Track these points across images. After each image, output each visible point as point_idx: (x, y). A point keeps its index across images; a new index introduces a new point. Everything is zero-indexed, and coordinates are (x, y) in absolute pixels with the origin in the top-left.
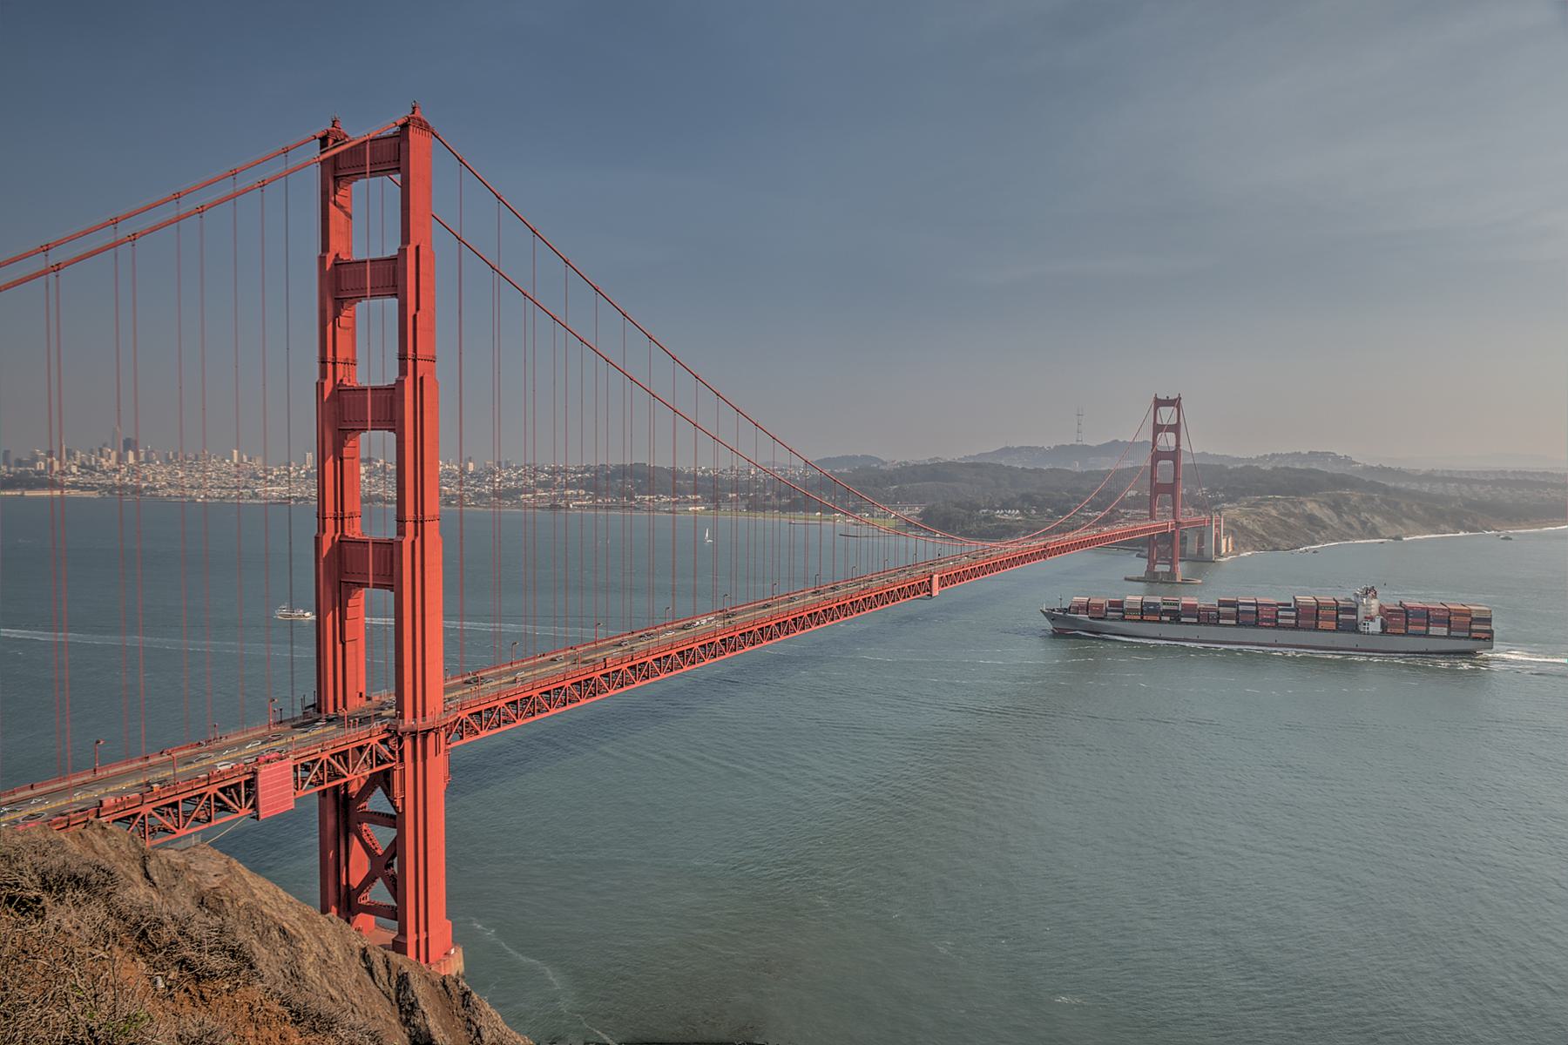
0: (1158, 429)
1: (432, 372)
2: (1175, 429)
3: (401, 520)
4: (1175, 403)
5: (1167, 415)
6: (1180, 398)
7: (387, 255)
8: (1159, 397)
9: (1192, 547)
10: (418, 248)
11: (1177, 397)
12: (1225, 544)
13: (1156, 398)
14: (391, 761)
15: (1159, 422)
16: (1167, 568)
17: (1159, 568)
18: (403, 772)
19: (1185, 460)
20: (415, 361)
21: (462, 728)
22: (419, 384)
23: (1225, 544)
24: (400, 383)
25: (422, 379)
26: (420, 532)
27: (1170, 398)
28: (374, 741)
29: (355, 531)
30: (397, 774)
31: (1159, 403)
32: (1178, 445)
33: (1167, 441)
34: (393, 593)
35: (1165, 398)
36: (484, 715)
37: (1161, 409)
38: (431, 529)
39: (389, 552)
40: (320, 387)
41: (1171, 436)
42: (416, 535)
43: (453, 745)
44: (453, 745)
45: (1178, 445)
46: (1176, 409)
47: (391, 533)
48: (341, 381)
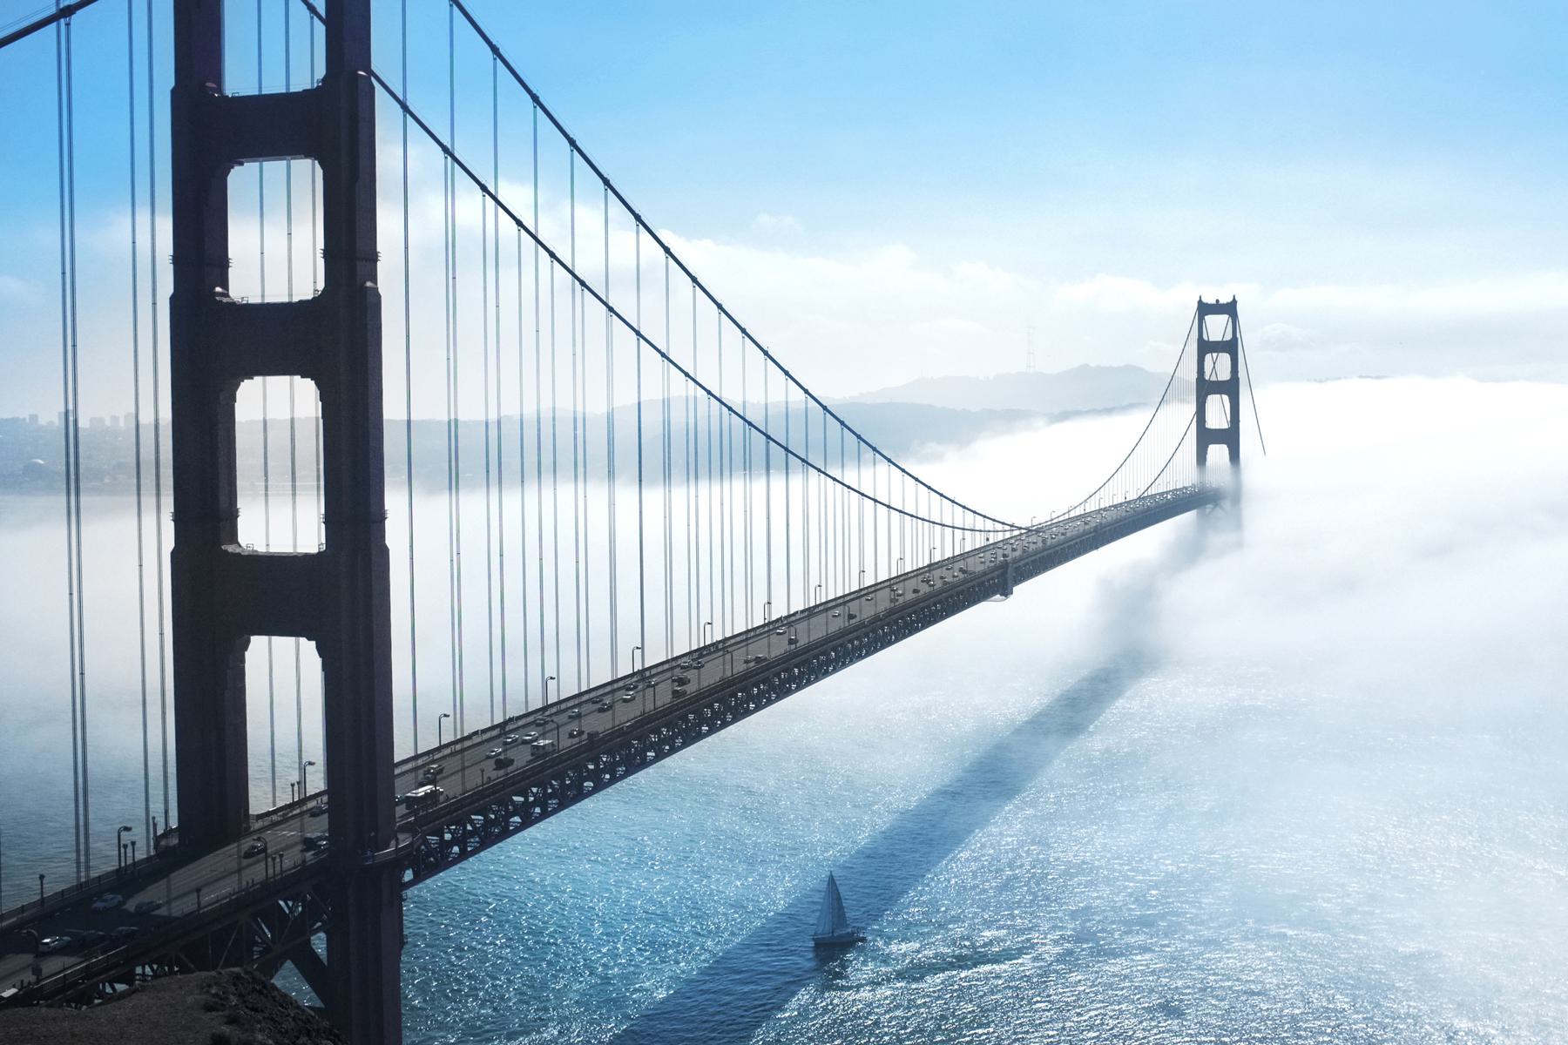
0: (1205, 347)
1: (373, 277)
2: (1230, 347)
3: (332, 519)
4: (1230, 309)
5: (1217, 327)
6: (1236, 302)
7: (296, 87)
8: (1204, 300)
11: (1230, 300)
13: (1200, 302)
15: (1206, 339)
27: (1223, 301)
31: (1204, 309)
33: (1219, 367)
34: (313, 643)
35: (1214, 302)
36: (448, 836)
37: (1210, 319)
41: (1225, 358)
46: (1230, 323)
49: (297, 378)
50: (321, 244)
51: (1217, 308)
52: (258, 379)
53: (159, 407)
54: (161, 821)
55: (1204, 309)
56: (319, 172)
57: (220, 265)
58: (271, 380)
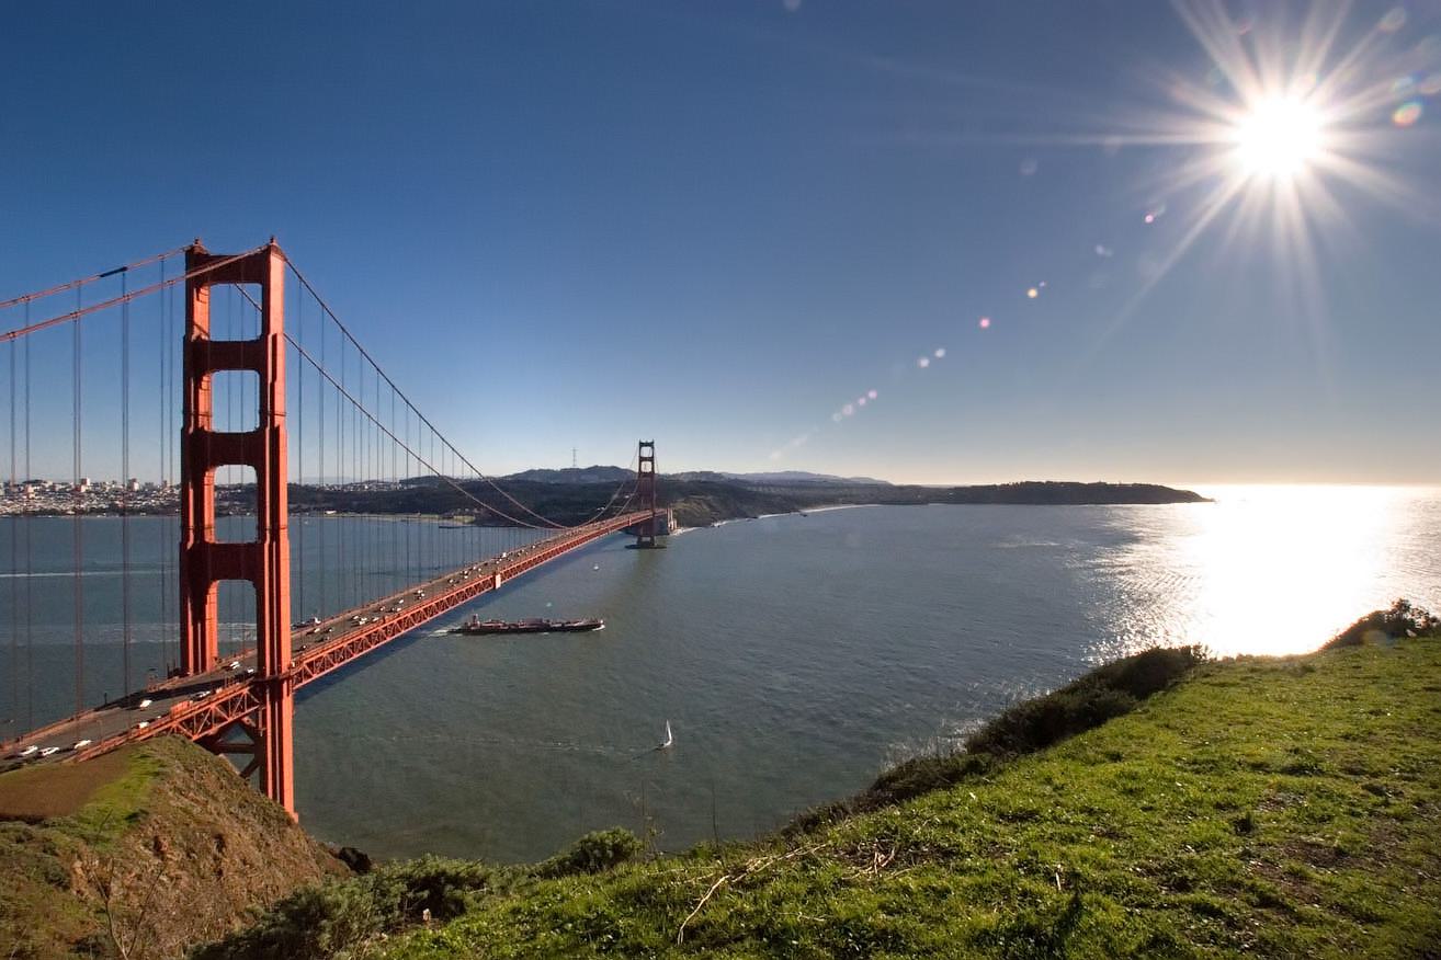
0: (642, 459)
2: (651, 459)
4: (651, 445)
5: (646, 452)
9: (656, 528)
10: (275, 337)
12: (672, 523)
14: (256, 704)
16: (649, 539)
17: (644, 539)
18: (265, 712)
19: (656, 478)
20: (273, 415)
21: (302, 675)
22: (275, 432)
23: (672, 523)
24: (260, 432)
25: (278, 427)
26: (275, 537)
27: (649, 441)
28: (246, 691)
29: (210, 538)
30: (260, 713)
31: (642, 445)
32: (653, 468)
33: (647, 467)
37: (643, 448)
38: (283, 534)
39: (256, 549)
40: (184, 431)
41: (650, 463)
42: (272, 539)
43: (297, 686)
44: (297, 686)
45: (653, 468)
47: (251, 537)
48: (203, 427)
49: (245, 466)
50: (258, 408)
51: (647, 445)
52: (226, 467)
53: (177, 479)
54: (171, 662)
55: (642, 445)
56: (258, 376)
57: (208, 415)
58: (232, 466)
